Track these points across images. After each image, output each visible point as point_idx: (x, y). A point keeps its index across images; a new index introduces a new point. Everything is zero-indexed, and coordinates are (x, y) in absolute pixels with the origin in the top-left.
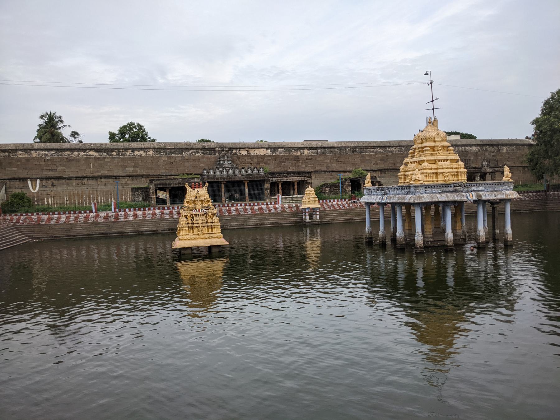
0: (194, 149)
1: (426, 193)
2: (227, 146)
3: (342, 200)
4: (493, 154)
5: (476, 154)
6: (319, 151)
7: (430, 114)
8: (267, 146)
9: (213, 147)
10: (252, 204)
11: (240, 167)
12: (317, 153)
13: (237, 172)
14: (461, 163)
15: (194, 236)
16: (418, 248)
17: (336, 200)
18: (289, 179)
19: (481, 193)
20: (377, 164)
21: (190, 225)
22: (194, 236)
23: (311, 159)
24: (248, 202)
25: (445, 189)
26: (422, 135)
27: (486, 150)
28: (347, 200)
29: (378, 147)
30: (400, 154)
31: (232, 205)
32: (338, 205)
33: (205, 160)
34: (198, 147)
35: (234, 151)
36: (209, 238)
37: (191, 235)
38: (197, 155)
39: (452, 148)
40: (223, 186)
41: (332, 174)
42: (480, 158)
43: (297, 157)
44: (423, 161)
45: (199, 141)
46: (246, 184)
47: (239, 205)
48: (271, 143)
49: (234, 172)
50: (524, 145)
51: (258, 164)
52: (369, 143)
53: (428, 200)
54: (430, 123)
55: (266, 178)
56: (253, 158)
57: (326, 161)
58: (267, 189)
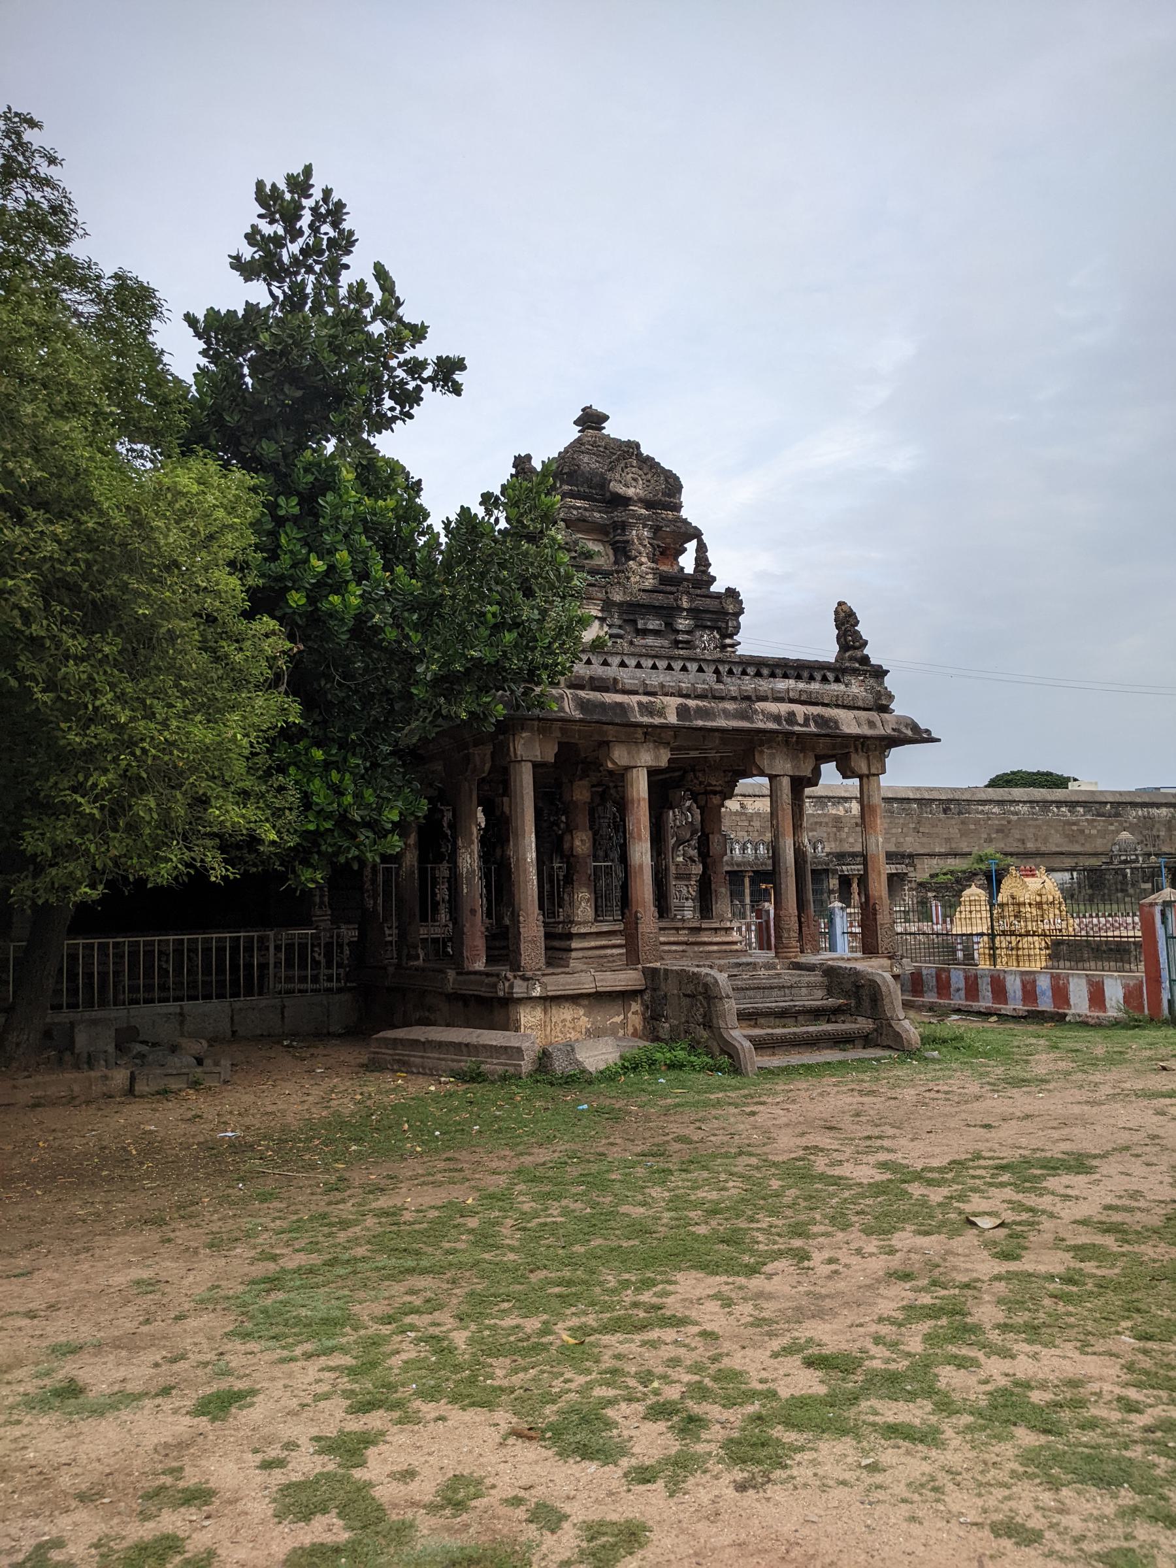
30: (1032, 819)
40: (747, 881)
43: (837, 819)
45: (1000, 781)
55: (831, 866)
57: (894, 831)
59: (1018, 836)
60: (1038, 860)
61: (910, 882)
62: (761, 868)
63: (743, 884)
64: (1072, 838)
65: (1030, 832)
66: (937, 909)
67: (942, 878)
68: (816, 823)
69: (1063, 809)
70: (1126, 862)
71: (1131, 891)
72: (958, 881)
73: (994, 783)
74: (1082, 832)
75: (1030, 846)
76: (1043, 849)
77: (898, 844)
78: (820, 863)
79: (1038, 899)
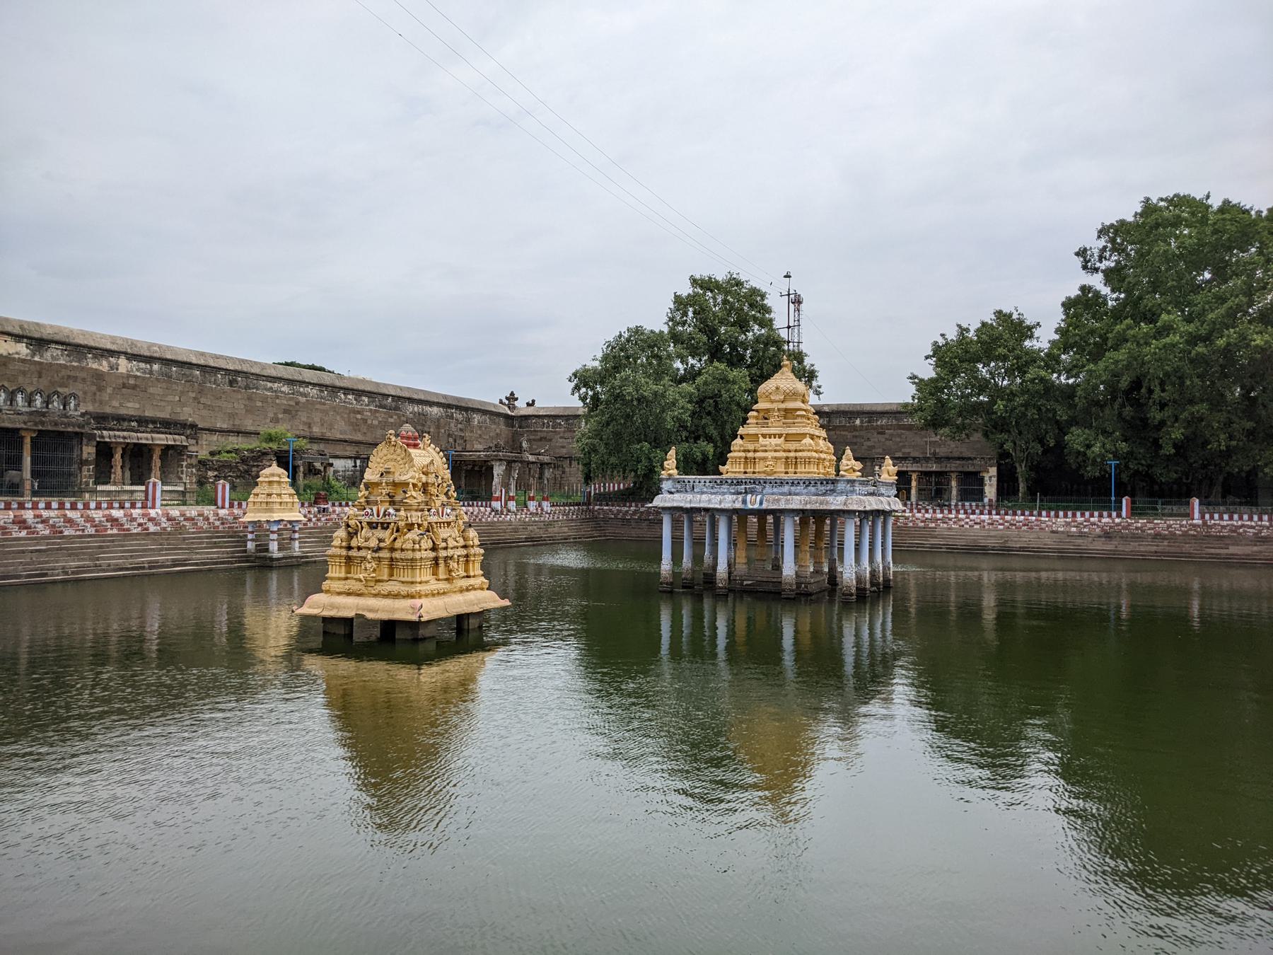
6: (156, 367)
8: (17, 331)
12: (151, 372)
18: (144, 438)
20: (276, 420)
23: (134, 387)
24: (27, 499)
27: (452, 417)
30: (320, 403)
37: (434, 586)
43: (99, 376)
44: (804, 435)
46: (28, 441)
47: (93, 505)
48: (28, 323)
50: (499, 415)
55: (87, 430)
57: (170, 398)
58: (87, 462)
59: (304, 419)
61: (190, 457)
64: (355, 426)
66: (223, 488)
67: (225, 457)
68: (69, 377)
72: (244, 461)
75: (316, 430)
76: (329, 435)
78: (68, 425)
79: (424, 479)
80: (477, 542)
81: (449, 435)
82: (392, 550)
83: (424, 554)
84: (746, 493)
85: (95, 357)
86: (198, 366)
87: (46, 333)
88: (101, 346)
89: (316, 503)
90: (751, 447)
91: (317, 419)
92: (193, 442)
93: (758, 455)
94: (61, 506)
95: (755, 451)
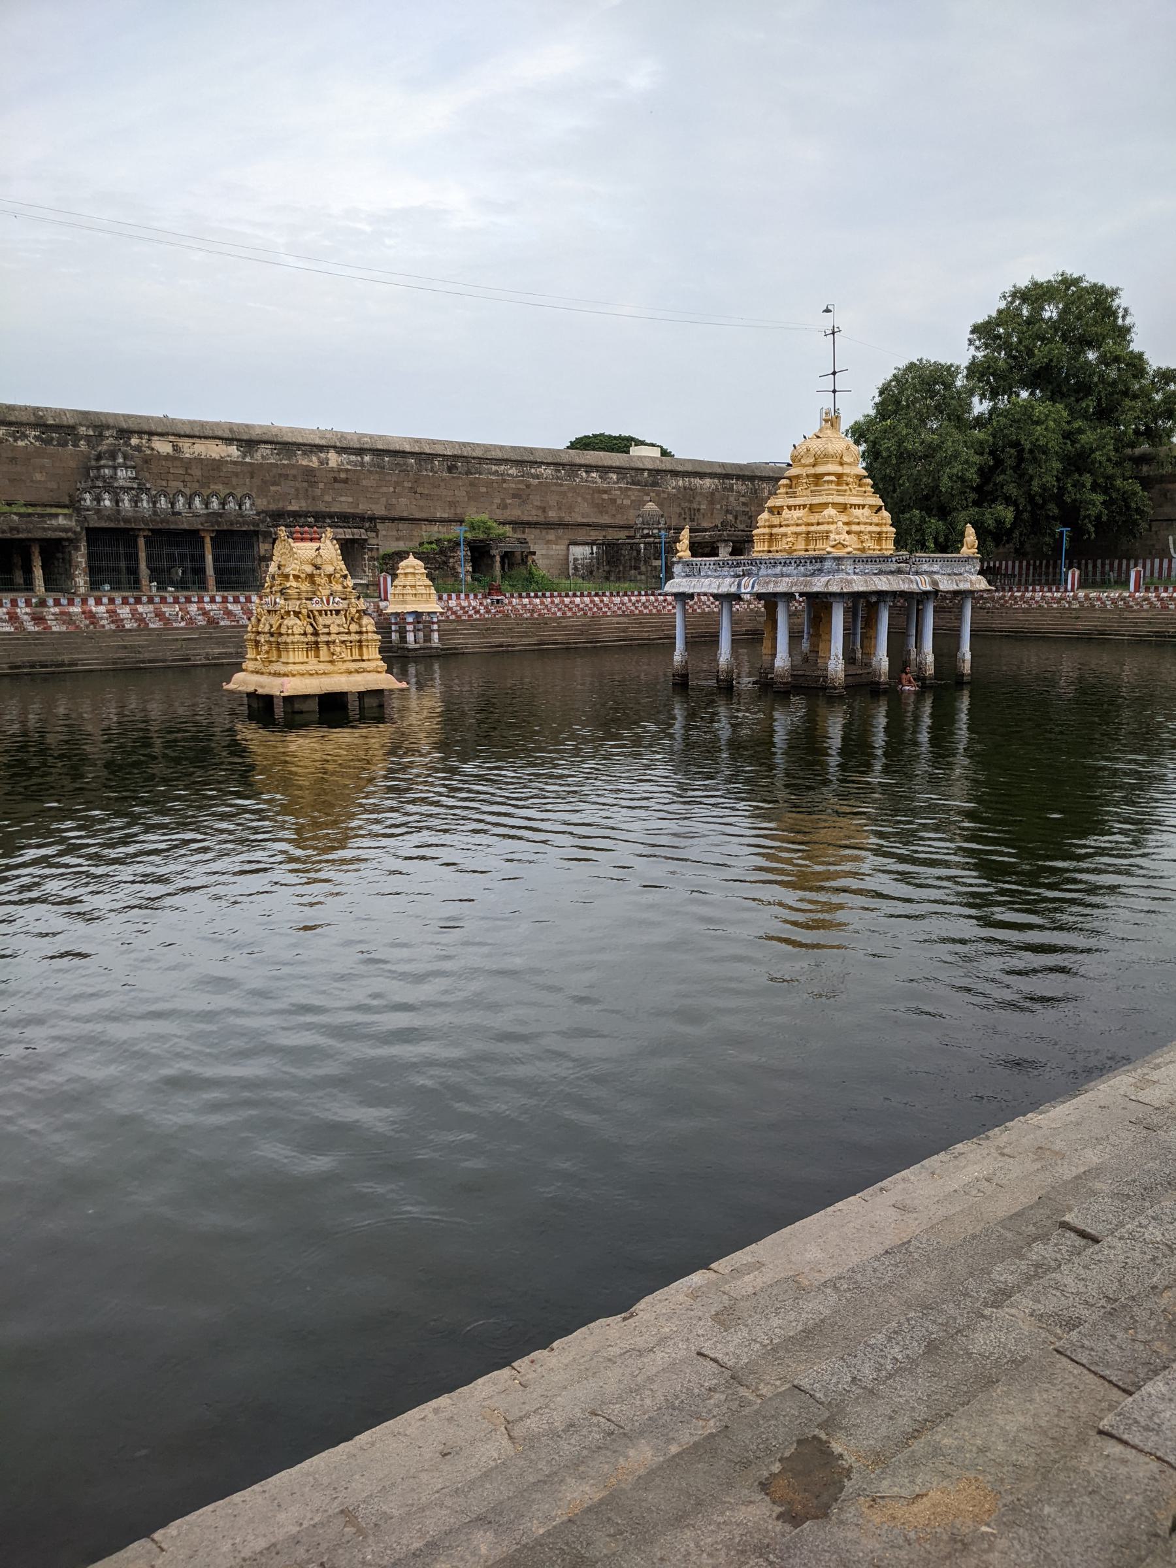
0: (11, 424)
1: (855, 573)
2: (111, 422)
3: (467, 596)
4: (742, 499)
5: (711, 496)
6: (367, 458)
7: (827, 401)
8: (227, 434)
9: (71, 422)
10: (242, 599)
11: (171, 492)
12: (362, 464)
13: (181, 503)
14: (885, 514)
15: (322, 667)
16: (835, 688)
17: (454, 596)
19: (936, 577)
20: (505, 507)
21: (311, 638)
22: (322, 667)
23: (346, 481)
25: (884, 567)
26: (816, 446)
27: (731, 489)
28: (480, 596)
29: (506, 461)
30: (556, 484)
31: (188, 600)
32: (463, 608)
33: (46, 462)
34: (24, 419)
35: (134, 441)
36: (358, 672)
37: (313, 665)
38: (20, 443)
39: (869, 481)
40: (141, 542)
41: (401, 526)
42: (718, 507)
43: (309, 472)
44: (826, 505)
46: (208, 541)
47: (231, 599)
49: (173, 504)
51: (203, 485)
52: (488, 448)
53: (861, 589)
54: (826, 421)
55: (262, 527)
56: (188, 464)
57: (385, 489)
59: (539, 504)
60: (561, 532)
61: (371, 550)
62: (160, 526)
63: (136, 546)
64: (601, 508)
65: (552, 500)
68: (280, 475)
69: (594, 475)
70: (648, 536)
71: (643, 569)
73: (573, 446)
74: (613, 501)
75: (552, 515)
76: (567, 519)
77: (389, 506)
78: (244, 523)
80: (372, 628)
81: (728, 512)
82: (281, 634)
83: (297, 638)
84: (744, 575)
85: (304, 453)
86: (412, 454)
87: (255, 434)
88: (310, 441)
89: (490, 594)
90: (776, 520)
91: (553, 503)
92: (373, 534)
93: (782, 530)
94: (225, 600)
95: (818, 524)
